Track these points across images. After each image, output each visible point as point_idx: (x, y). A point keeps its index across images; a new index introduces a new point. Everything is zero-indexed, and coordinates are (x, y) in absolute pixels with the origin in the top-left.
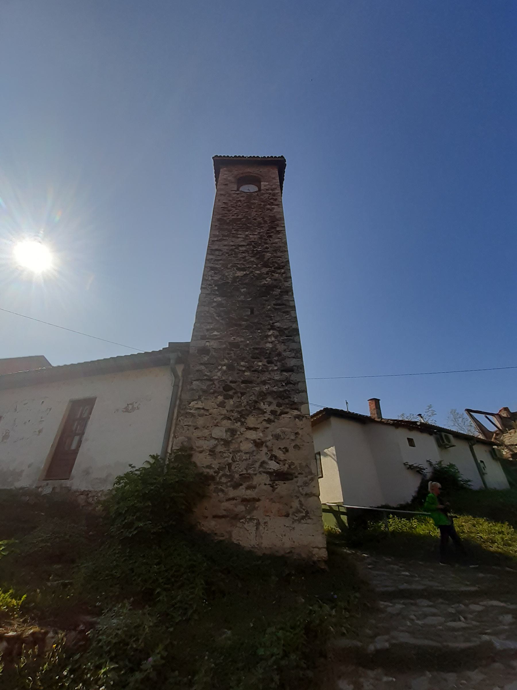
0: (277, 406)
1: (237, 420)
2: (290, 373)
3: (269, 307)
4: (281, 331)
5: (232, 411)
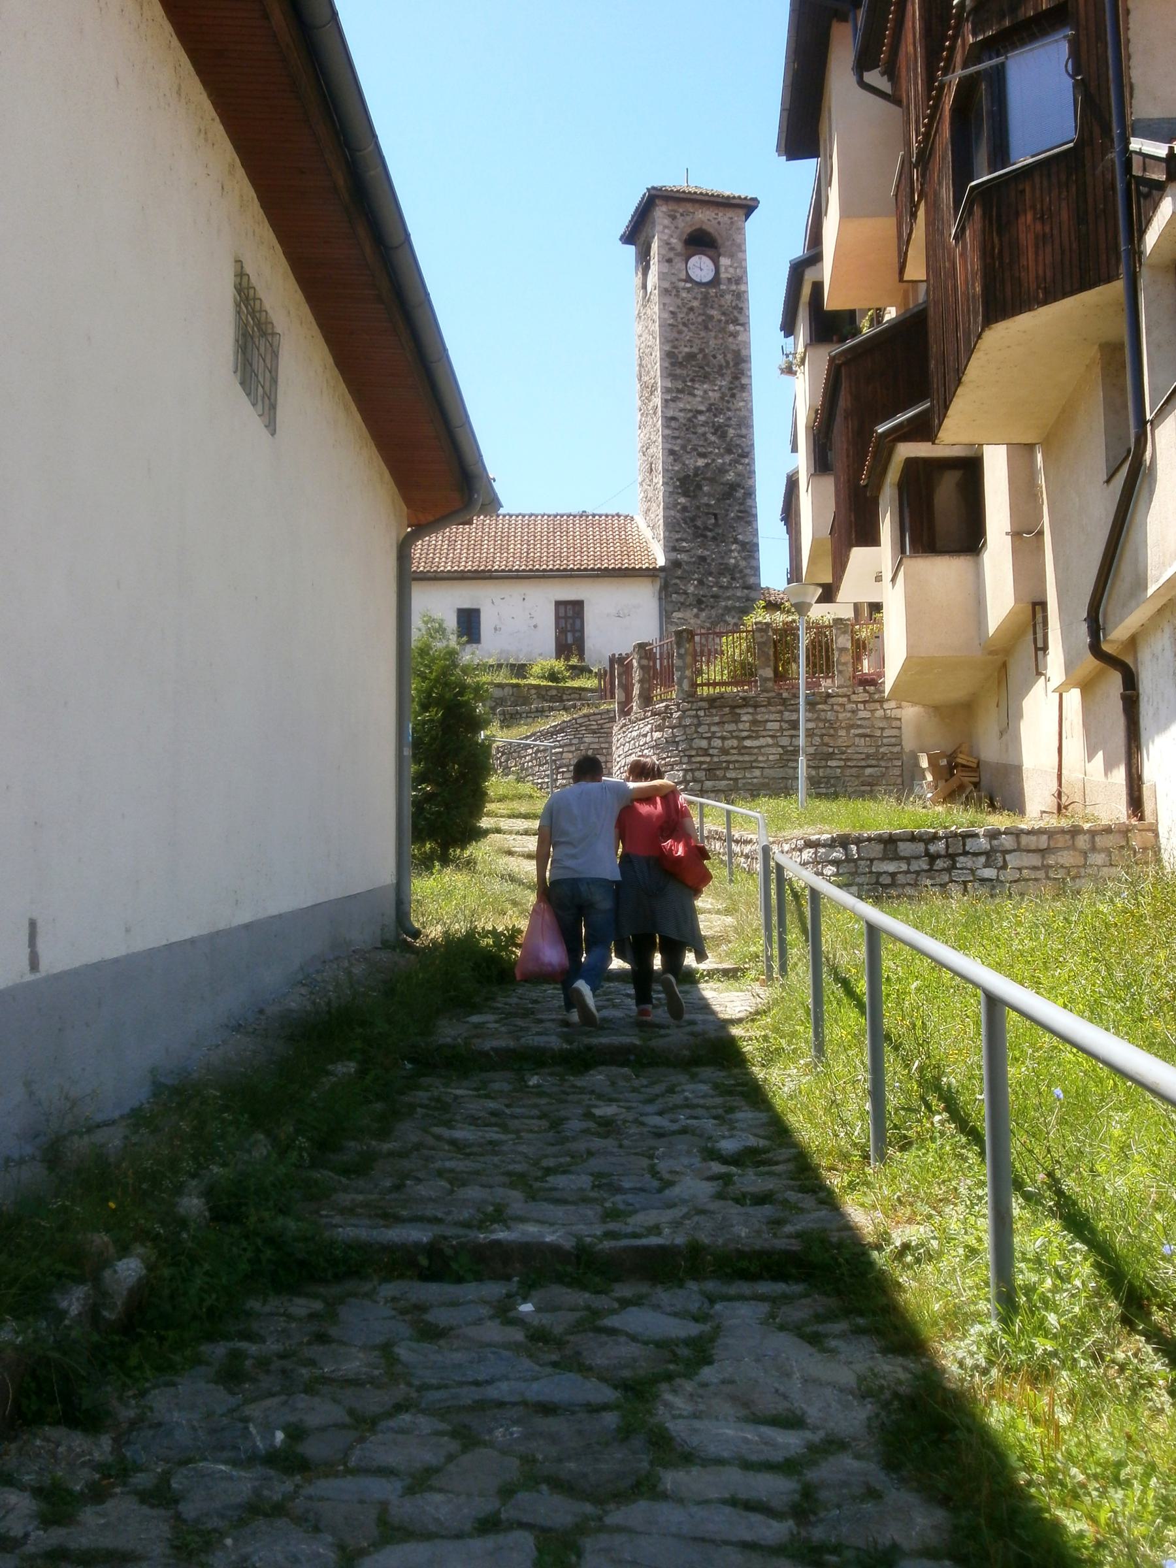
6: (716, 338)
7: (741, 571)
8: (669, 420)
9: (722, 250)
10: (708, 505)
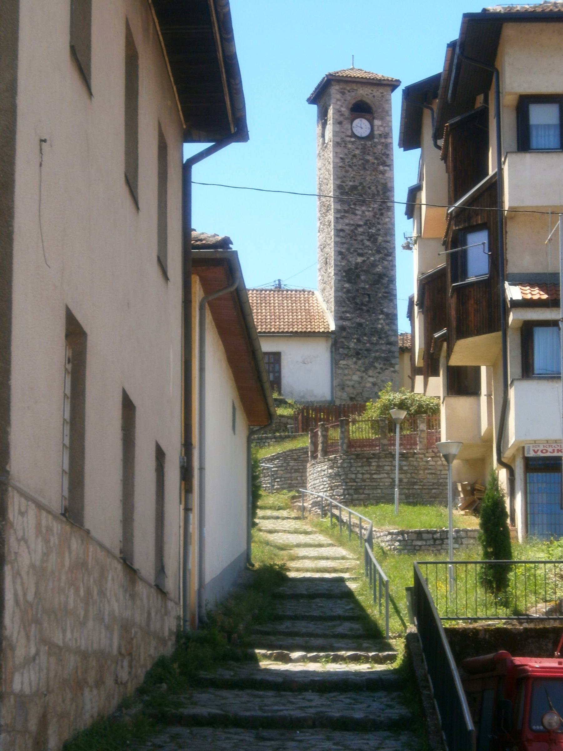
1: (364, 372)
3: (380, 295)
5: (360, 367)
6: (371, 175)
7: (385, 333)
8: (338, 232)
9: (375, 115)
10: (364, 288)
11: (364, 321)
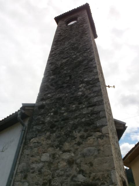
0: (84, 132)
1: (57, 147)
2: (94, 107)
3: (80, 72)
4: (88, 83)
11: (63, 94)
